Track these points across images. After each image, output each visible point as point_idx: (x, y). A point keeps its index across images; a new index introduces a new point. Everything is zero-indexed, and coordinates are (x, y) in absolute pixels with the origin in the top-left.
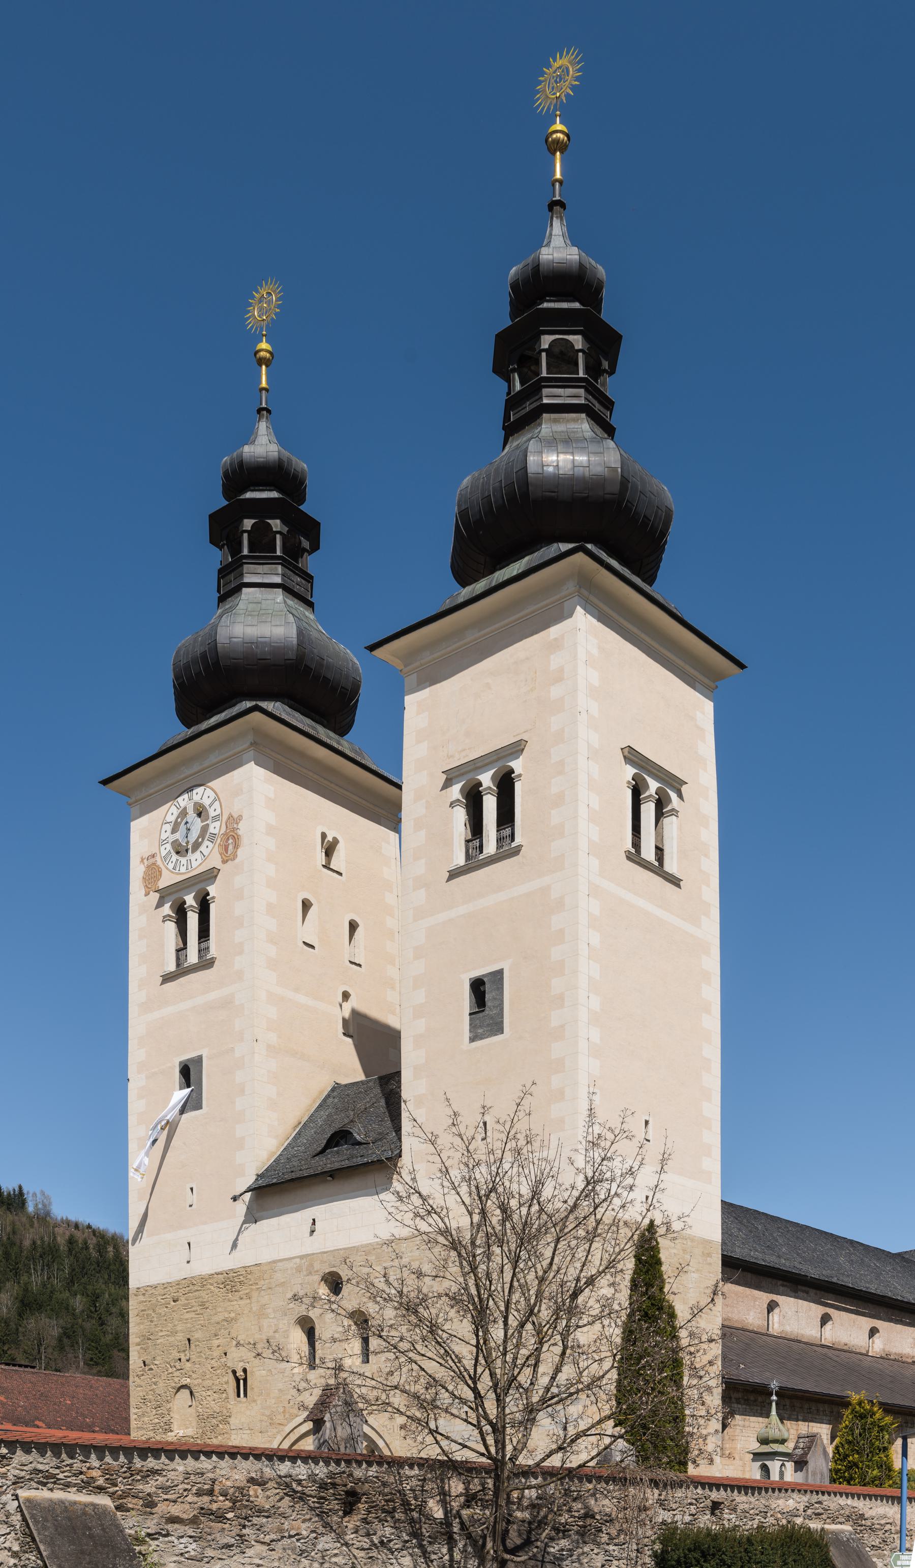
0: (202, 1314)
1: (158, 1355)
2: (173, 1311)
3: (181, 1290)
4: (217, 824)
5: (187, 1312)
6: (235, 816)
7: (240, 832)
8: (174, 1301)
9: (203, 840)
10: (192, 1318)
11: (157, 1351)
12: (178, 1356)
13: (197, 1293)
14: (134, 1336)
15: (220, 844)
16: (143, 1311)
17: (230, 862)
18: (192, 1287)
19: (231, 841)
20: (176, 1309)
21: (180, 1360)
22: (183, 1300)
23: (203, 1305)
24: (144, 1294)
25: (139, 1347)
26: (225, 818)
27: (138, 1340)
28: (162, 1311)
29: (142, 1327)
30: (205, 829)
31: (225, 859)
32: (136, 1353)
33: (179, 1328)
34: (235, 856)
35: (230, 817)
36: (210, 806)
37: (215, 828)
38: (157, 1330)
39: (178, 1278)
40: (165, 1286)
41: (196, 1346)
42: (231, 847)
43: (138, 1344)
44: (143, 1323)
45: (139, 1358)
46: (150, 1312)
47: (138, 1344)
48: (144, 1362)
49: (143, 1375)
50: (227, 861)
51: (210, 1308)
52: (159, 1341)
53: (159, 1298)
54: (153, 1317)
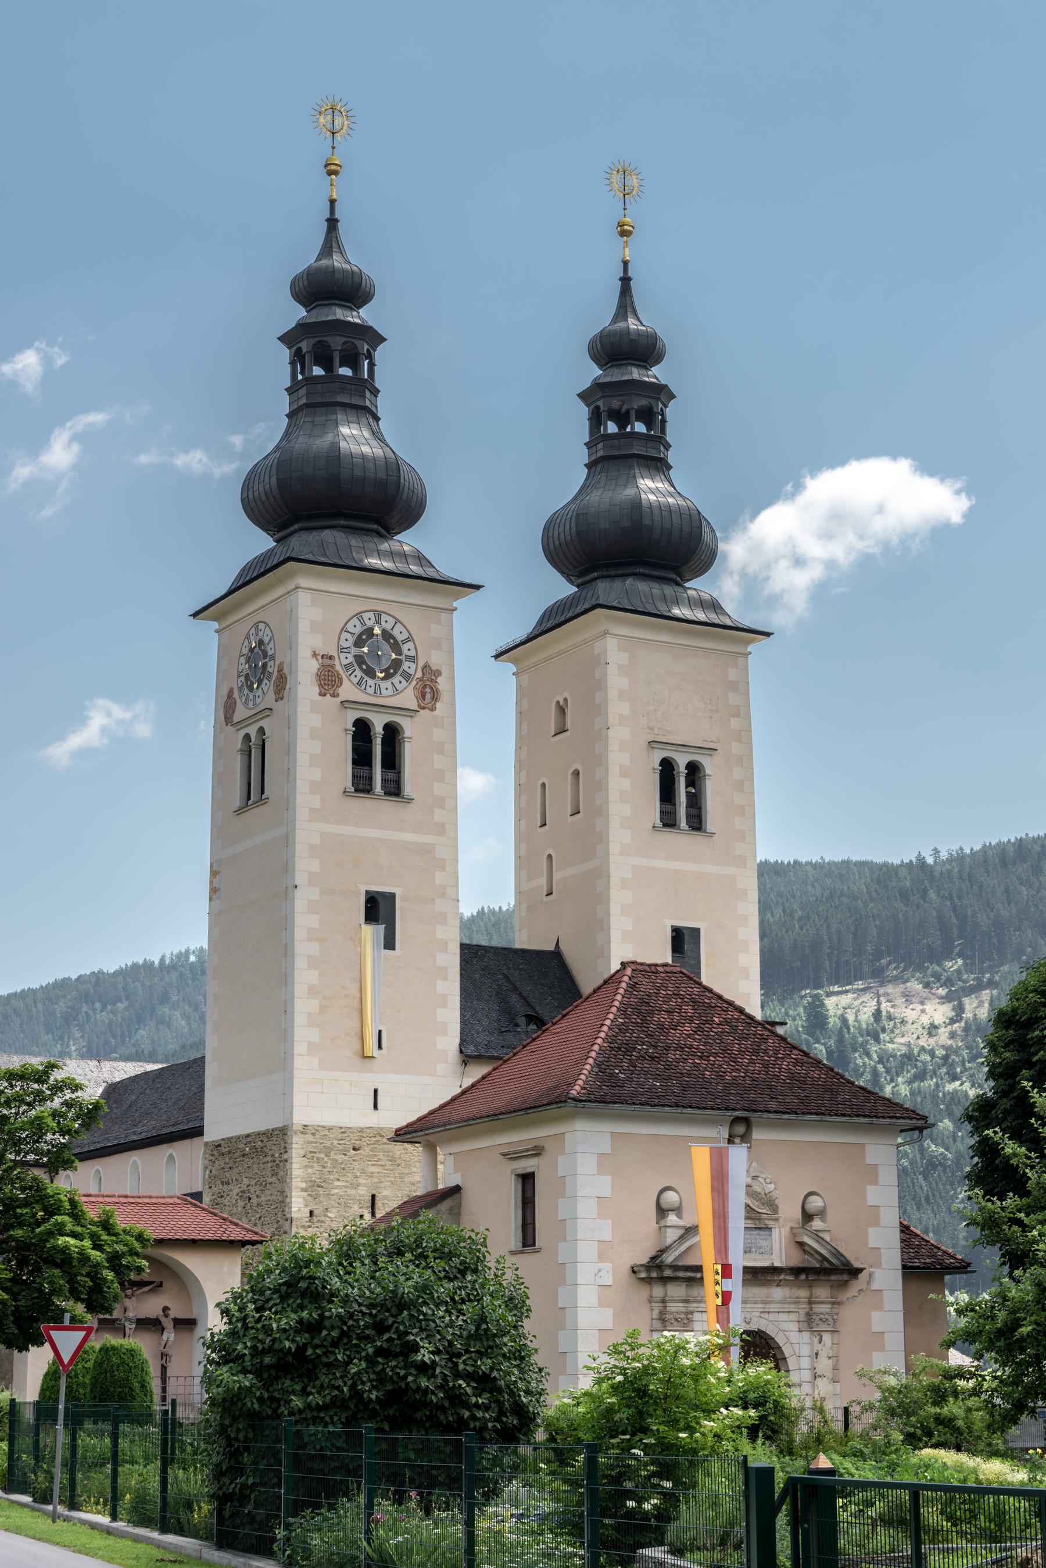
0: (392, 1170)
1: (333, 1207)
2: (354, 1161)
3: (366, 1139)
4: (413, 666)
5: (373, 1165)
6: (434, 668)
7: (440, 687)
8: (354, 1149)
9: (395, 673)
10: (378, 1173)
11: (332, 1202)
12: (360, 1212)
13: (385, 1146)
14: (299, 1179)
15: (415, 687)
16: (311, 1152)
17: (426, 710)
18: (378, 1138)
19: (428, 690)
20: (357, 1158)
21: (361, 1216)
22: (366, 1151)
23: (393, 1159)
24: (313, 1134)
25: (305, 1194)
26: (421, 664)
27: (303, 1185)
28: (340, 1158)
29: (310, 1171)
30: (396, 664)
31: (422, 705)
32: (301, 1200)
33: (361, 1181)
34: (433, 709)
35: (426, 667)
36: (404, 642)
37: (406, 666)
38: (332, 1177)
39: (362, 1125)
40: (344, 1130)
41: (383, 1204)
42: (428, 696)
43: (304, 1190)
44: (312, 1167)
45: (306, 1206)
46: (322, 1156)
47: (304, 1190)
48: (311, 1213)
49: (310, 1227)
50: (424, 708)
51: (403, 1165)
52: (334, 1191)
53: (335, 1142)
54: (326, 1162)
